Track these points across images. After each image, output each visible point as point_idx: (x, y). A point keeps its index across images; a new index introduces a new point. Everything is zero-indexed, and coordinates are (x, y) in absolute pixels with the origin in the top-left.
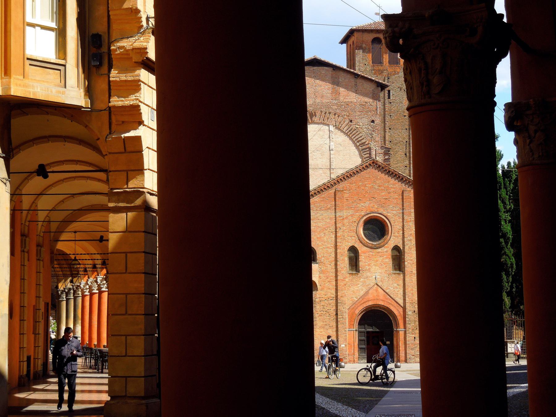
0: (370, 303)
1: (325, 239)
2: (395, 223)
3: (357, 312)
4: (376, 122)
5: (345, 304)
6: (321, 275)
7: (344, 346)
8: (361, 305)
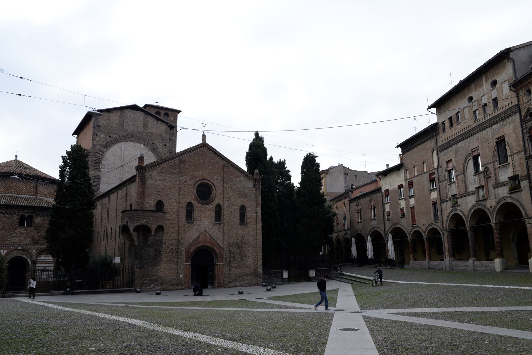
0: (201, 244)
1: (171, 195)
2: (218, 188)
3: (192, 251)
4: (167, 146)
5: (183, 245)
6: (167, 222)
7: (182, 276)
8: (195, 245)
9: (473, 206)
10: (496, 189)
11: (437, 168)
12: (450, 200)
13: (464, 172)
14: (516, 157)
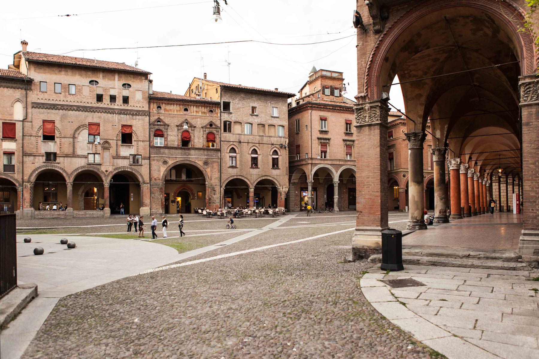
9: (83, 167)
10: (115, 160)
11: (23, 121)
12: (43, 156)
13: (74, 137)
14: (141, 143)
